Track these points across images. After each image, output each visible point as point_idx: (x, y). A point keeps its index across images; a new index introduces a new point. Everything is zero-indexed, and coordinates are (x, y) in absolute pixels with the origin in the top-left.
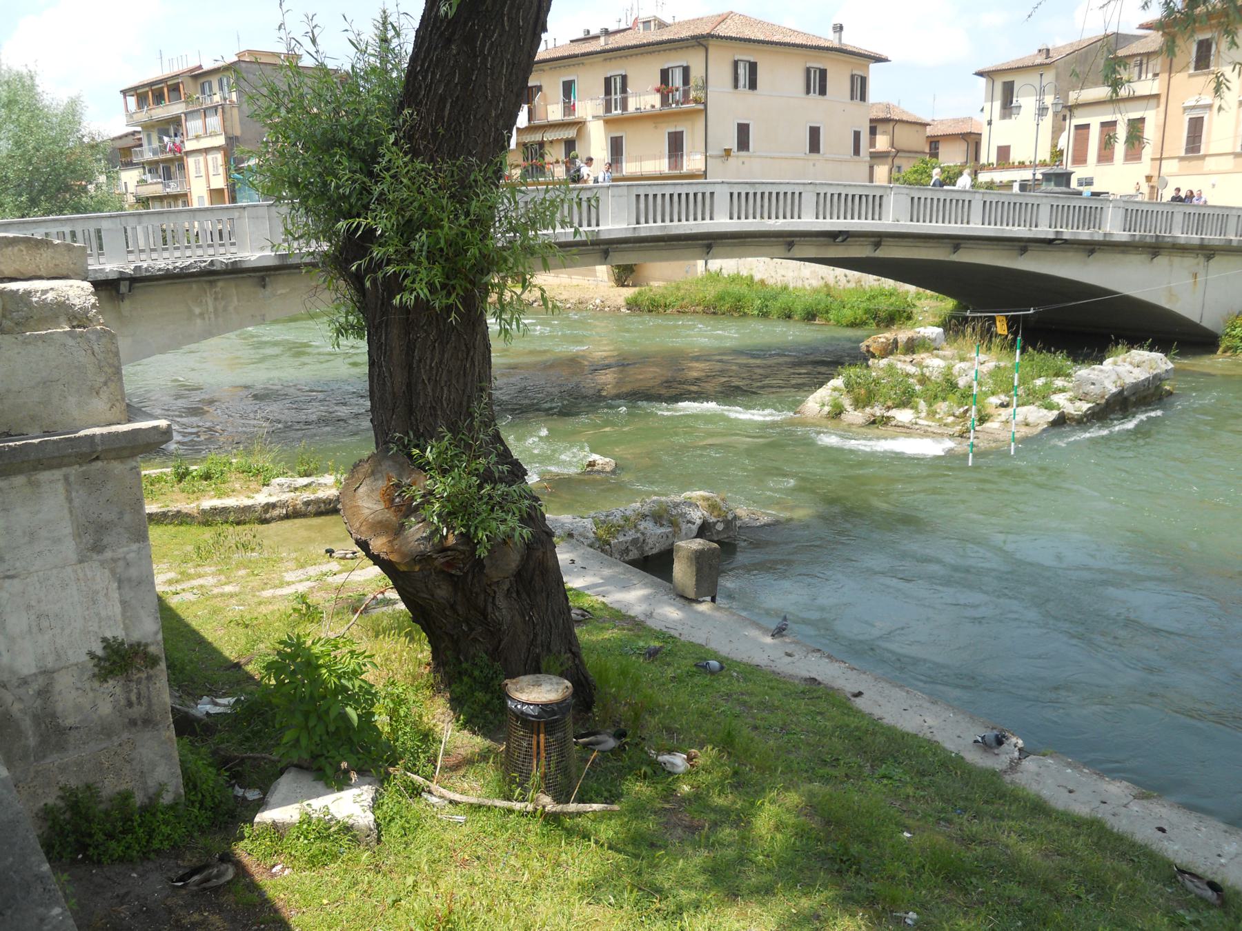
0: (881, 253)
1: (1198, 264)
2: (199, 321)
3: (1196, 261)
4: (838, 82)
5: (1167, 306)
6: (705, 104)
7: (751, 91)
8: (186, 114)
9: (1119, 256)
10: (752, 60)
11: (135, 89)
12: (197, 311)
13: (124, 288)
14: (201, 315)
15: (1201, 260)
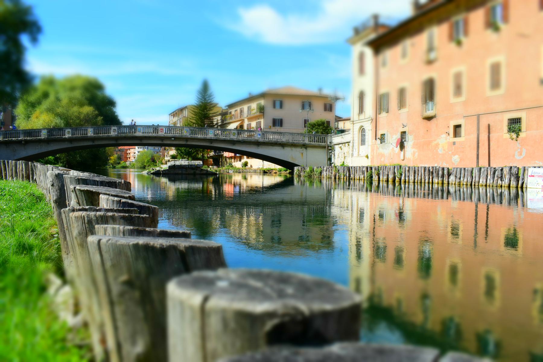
0: (189, 143)
1: (303, 150)
2: (37, 150)
3: (302, 149)
4: (318, 107)
5: (292, 162)
6: (263, 113)
7: (280, 109)
8: (177, 120)
9: (271, 147)
10: (281, 100)
11: (171, 114)
12: (37, 148)
13: (23, 142)
14: (38, 149)
15: (304, 149)
